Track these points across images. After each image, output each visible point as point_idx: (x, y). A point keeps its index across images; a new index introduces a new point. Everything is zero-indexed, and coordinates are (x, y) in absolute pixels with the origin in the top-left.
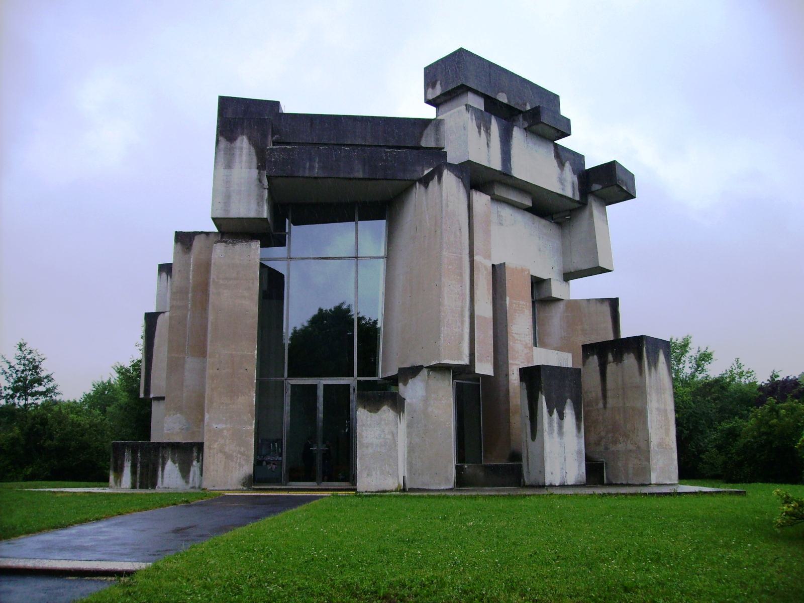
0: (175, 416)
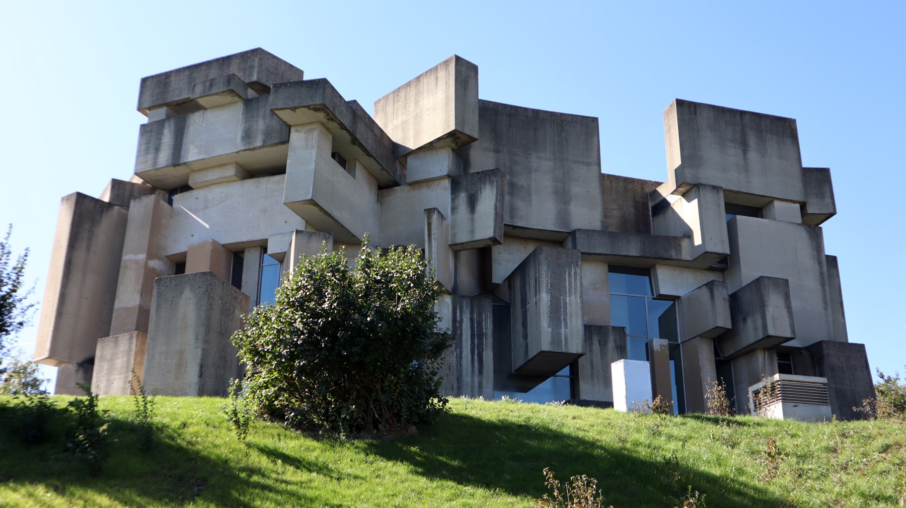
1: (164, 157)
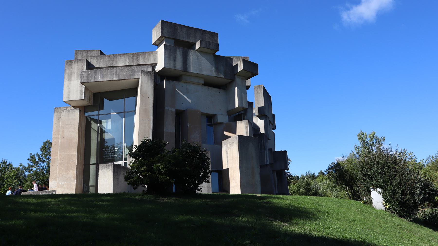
0: (54, 182)
1: (179, 66)
